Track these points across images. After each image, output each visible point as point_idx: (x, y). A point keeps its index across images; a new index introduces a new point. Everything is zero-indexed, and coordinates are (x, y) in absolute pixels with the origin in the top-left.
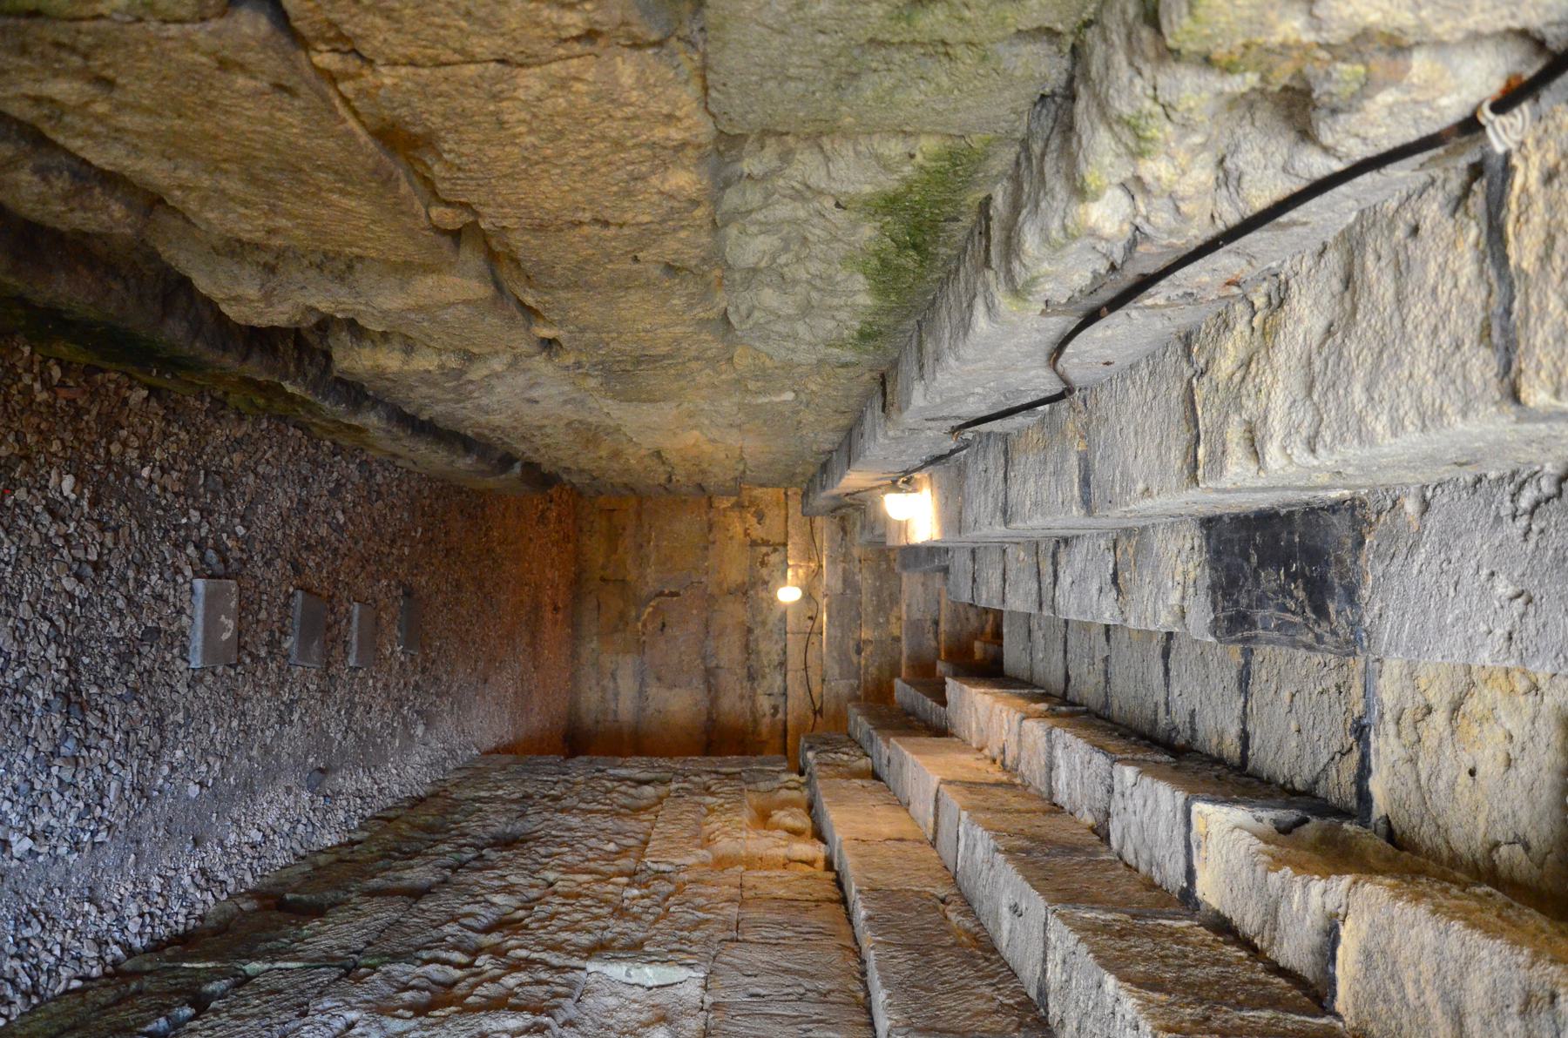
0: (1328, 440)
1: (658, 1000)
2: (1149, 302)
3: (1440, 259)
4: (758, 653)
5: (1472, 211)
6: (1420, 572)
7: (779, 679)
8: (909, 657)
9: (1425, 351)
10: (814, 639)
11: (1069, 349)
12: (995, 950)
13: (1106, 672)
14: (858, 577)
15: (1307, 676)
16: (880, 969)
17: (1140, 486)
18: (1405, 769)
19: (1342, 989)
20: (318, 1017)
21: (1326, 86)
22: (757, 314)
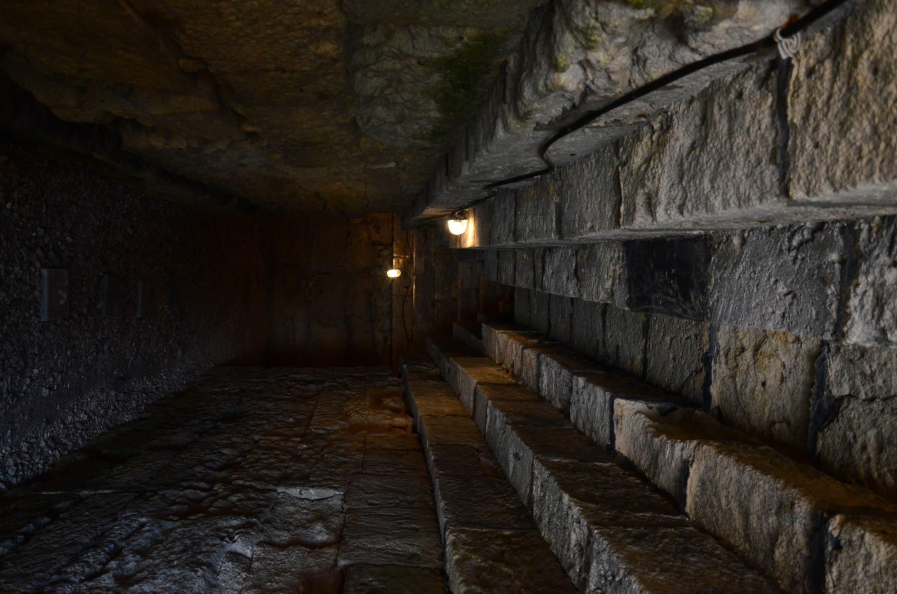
0: (690, 207)
1: (318, 507)
2: (595, 124)
3: (752, 113)
5: (770, 87)
6: (739, 277)
9: (742, 163)
11: (551, 148)
12: (505, 478)
13: (571, 323)
14: (433, 264)
15: (680, 329)
16: (441, 489)
17: (589, 225)
18: (729, 381)
19: (689, 500)
20: (123, 522)
21: (691, 17)
22: (373, 120)
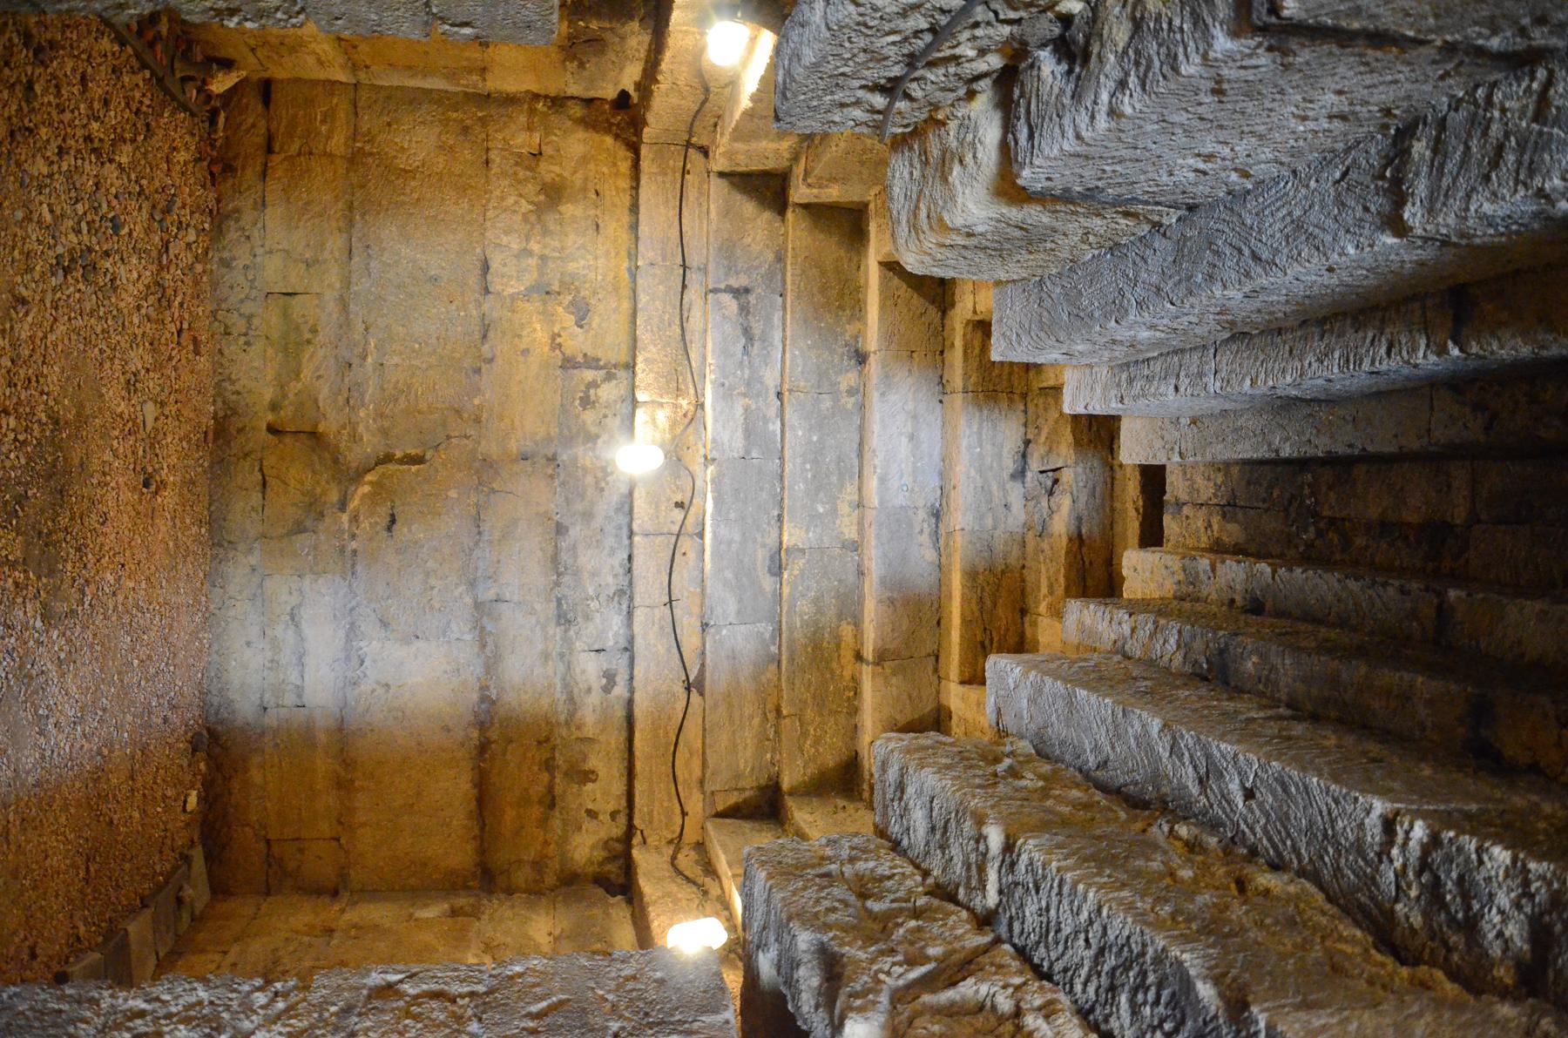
4: (577, 573)
7: (617, 621)
8: (883, 581)
10: (686, 544)
